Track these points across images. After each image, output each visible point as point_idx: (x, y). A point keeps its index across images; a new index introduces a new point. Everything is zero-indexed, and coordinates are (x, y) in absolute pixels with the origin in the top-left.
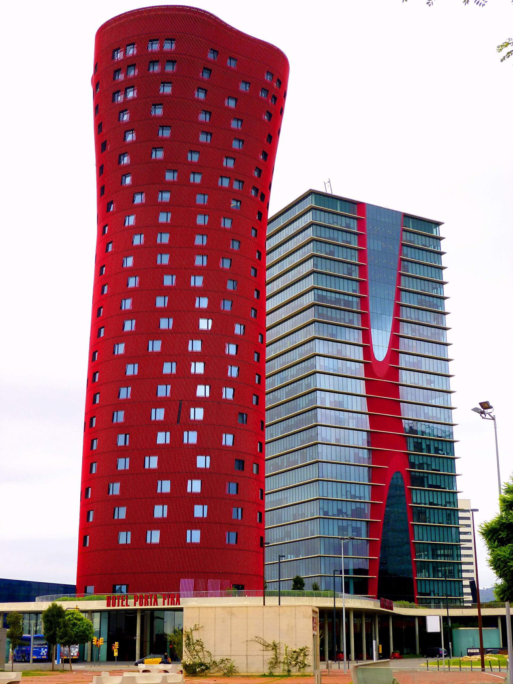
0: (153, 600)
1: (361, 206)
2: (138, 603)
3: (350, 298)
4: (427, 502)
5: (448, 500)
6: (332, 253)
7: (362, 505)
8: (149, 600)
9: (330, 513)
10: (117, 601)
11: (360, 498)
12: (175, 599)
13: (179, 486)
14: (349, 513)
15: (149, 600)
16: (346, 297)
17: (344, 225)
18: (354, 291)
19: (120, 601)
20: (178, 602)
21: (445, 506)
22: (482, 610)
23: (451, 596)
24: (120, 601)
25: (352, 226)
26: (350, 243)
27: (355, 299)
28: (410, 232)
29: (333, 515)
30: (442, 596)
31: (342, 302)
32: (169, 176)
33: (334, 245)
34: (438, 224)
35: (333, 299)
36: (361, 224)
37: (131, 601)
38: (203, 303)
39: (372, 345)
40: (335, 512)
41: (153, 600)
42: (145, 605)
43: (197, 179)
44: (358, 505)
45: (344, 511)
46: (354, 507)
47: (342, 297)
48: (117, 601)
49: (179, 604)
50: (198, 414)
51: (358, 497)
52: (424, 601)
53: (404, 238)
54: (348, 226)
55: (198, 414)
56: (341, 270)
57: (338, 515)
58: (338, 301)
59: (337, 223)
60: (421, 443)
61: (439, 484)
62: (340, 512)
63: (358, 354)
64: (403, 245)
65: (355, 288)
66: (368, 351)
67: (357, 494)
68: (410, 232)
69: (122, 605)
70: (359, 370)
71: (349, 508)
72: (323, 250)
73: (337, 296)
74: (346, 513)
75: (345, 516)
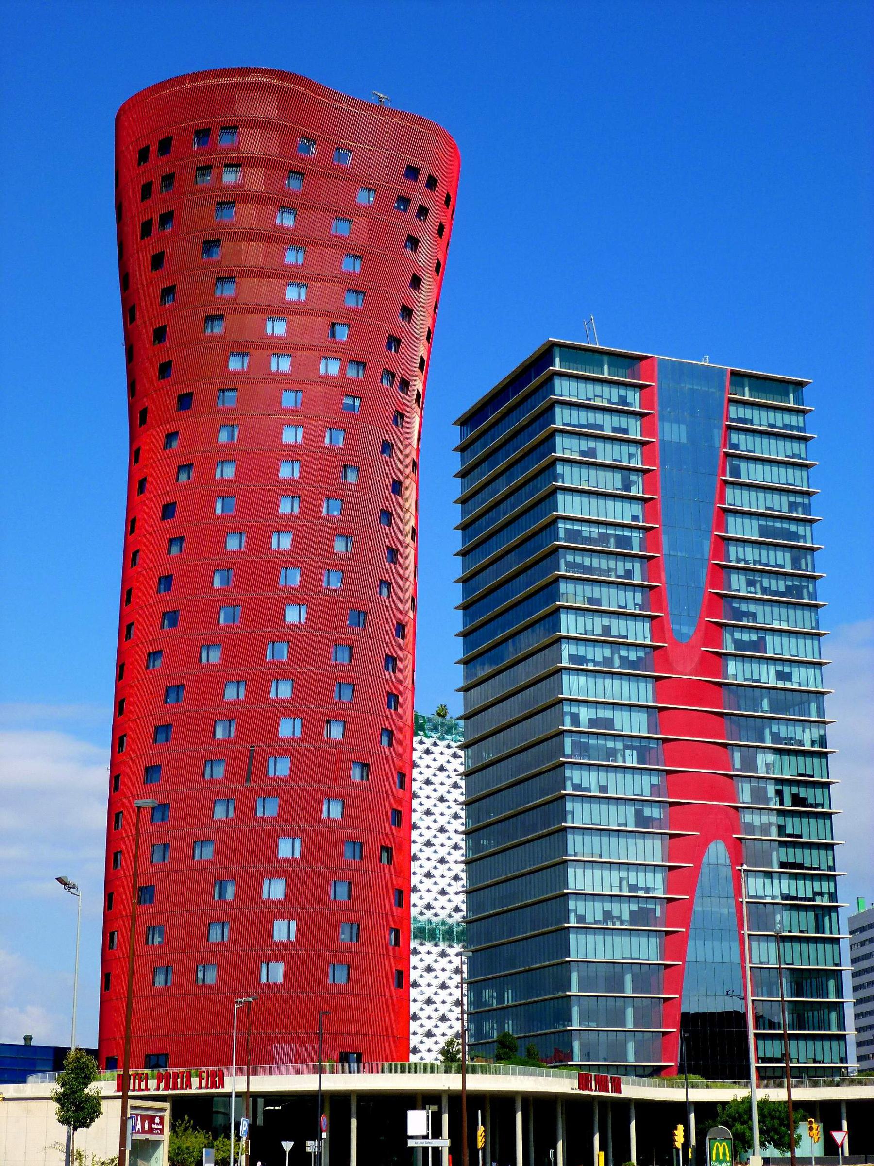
0: (185, 1079)
2: (162, 1085)
4: (777, 893)
5: (817, 889)
6: (592, 452)
8: (179, 1080)
9: (589, 918)
10: (132, 1082)
11: (647, 890)
12: (217, 1079)
13: (250, 889)
14: (626, 916)
15: (179, 1080)
17: (616, 400)
18: (635, 518)
19: (137, 1081)
20: (222, 1084)
21: (813, 900)
22: (793, 1090)
23: (823, 1062)
24: (137, 1081)
25: (630, 400)
26: (625, 431)
28: (745, 403)
29: (596, 922)
30: (806, 1063)
31: (612, 541)
32: (235, 364)
33: (596, 437)
35: (595, 535)
37: (152, 1083)
38: (294, 578)
39: (667, 614)
40: (599, 916)
41: (185, 1079)
42: (173, 1089)
43: (284, 365)
45: (615, 913)
46: (634, 907)
48: (132, 1082)
49: (223, 1087)
50: (281, 768)
51: (641, 889)
52: (820, 1073)
53: (733, 415)
54: (623, 400)
55: (281, 768)
56: (611, 482)
57: (605, 921)
58: (604, 538)
59: (601, 397)
60: (766, 788)
61: (799, 861)
62: (608, 916)
64: (729, 427)
67: (641, 884)
68: (745, 403)
69: (140, 1089)
71: (624, 910)
72: (575, 448)
74: (619, 918)
75: (618, 923)
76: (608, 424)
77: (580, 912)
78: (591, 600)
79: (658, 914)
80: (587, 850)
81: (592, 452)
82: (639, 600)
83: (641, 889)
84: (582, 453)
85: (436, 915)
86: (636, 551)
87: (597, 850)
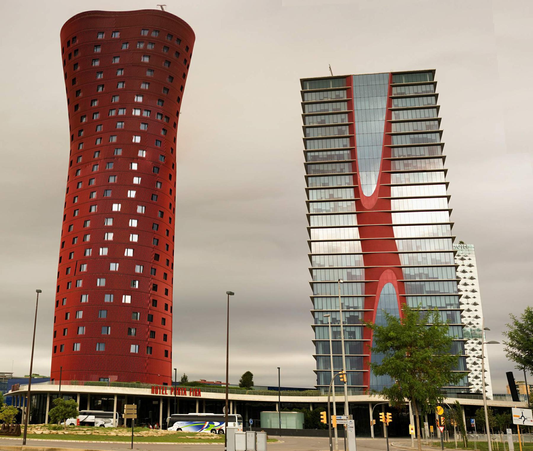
1: (348, 79)
3: (341, 152)
7: (356, 314)
16: (337, 152)
25: (341, 96)
27: (346, 152)
31: (336, 157)
34: (432, 72)
36: (349, 92)
44: (352, 314)
47: (333, 153)
51: (352, 307)
56: (335, 132)
63: (350, 194)
65: (345, 143)
66: (357, 190)
67: (351, 305)
70: (351, 207)
73: (329, 153)
76: (330, 108)
77: (321, 319)
78: (324, 184)
79: (360, 318)
80: (324, 291)
81: (324, 121)
82: (348, 181)
83: (352, 307)
84: (319, 123)
85: (474, 327)
86: (346, 159)
87: (328, 291)
